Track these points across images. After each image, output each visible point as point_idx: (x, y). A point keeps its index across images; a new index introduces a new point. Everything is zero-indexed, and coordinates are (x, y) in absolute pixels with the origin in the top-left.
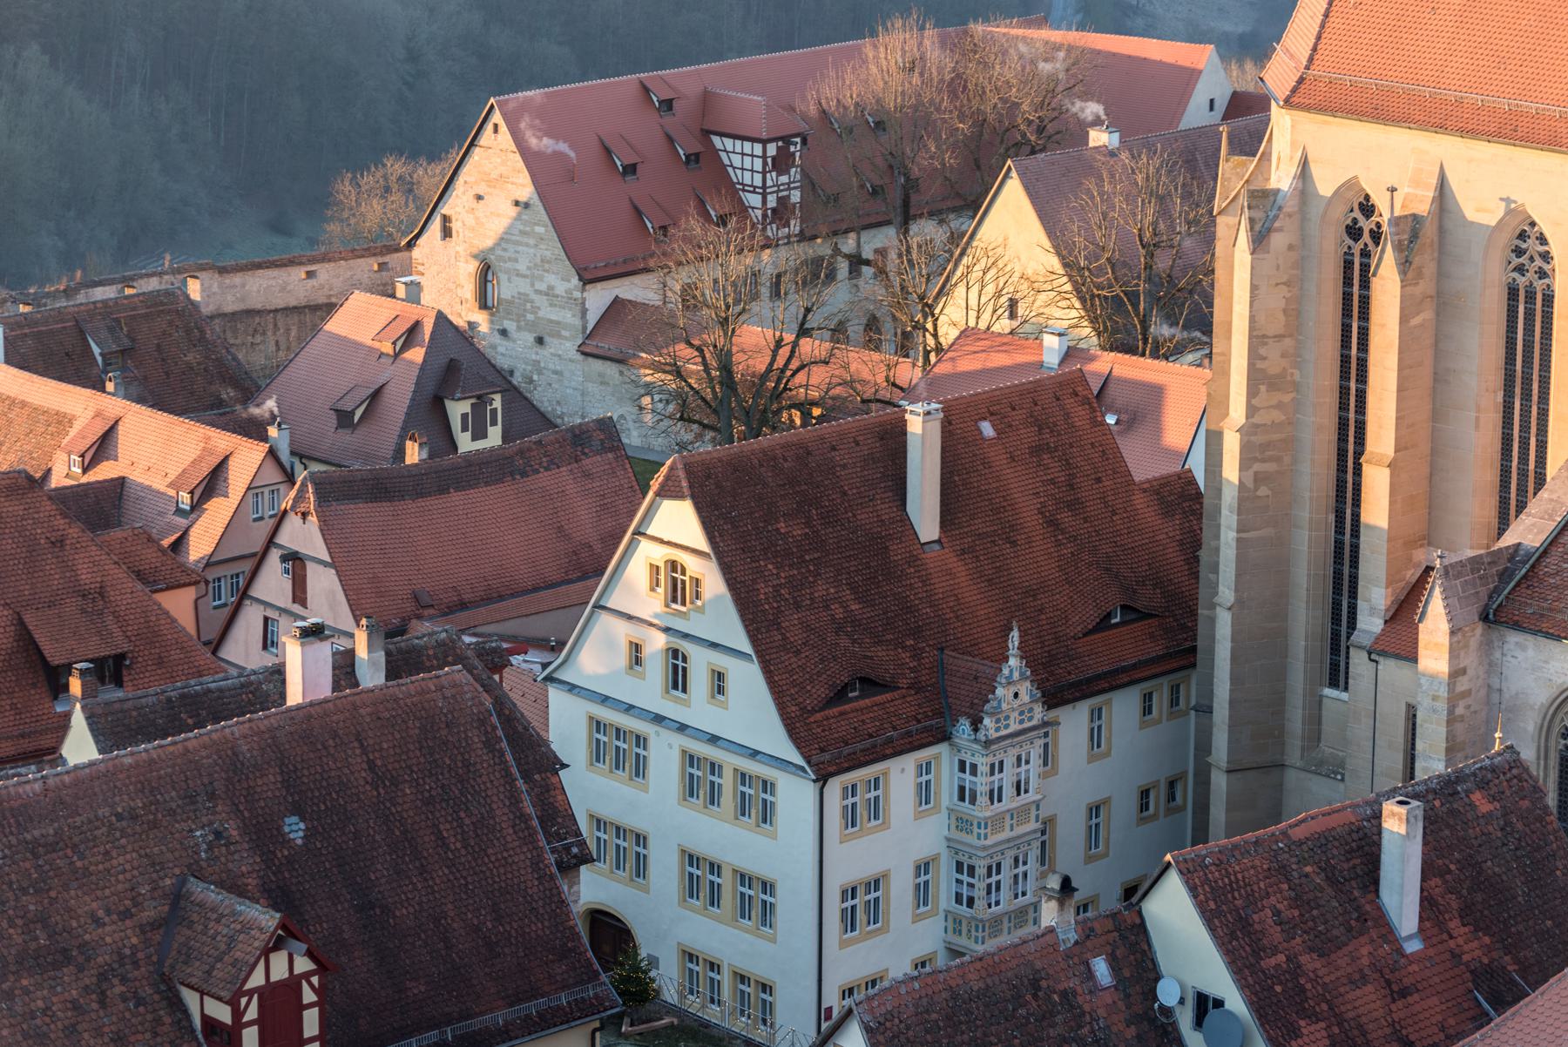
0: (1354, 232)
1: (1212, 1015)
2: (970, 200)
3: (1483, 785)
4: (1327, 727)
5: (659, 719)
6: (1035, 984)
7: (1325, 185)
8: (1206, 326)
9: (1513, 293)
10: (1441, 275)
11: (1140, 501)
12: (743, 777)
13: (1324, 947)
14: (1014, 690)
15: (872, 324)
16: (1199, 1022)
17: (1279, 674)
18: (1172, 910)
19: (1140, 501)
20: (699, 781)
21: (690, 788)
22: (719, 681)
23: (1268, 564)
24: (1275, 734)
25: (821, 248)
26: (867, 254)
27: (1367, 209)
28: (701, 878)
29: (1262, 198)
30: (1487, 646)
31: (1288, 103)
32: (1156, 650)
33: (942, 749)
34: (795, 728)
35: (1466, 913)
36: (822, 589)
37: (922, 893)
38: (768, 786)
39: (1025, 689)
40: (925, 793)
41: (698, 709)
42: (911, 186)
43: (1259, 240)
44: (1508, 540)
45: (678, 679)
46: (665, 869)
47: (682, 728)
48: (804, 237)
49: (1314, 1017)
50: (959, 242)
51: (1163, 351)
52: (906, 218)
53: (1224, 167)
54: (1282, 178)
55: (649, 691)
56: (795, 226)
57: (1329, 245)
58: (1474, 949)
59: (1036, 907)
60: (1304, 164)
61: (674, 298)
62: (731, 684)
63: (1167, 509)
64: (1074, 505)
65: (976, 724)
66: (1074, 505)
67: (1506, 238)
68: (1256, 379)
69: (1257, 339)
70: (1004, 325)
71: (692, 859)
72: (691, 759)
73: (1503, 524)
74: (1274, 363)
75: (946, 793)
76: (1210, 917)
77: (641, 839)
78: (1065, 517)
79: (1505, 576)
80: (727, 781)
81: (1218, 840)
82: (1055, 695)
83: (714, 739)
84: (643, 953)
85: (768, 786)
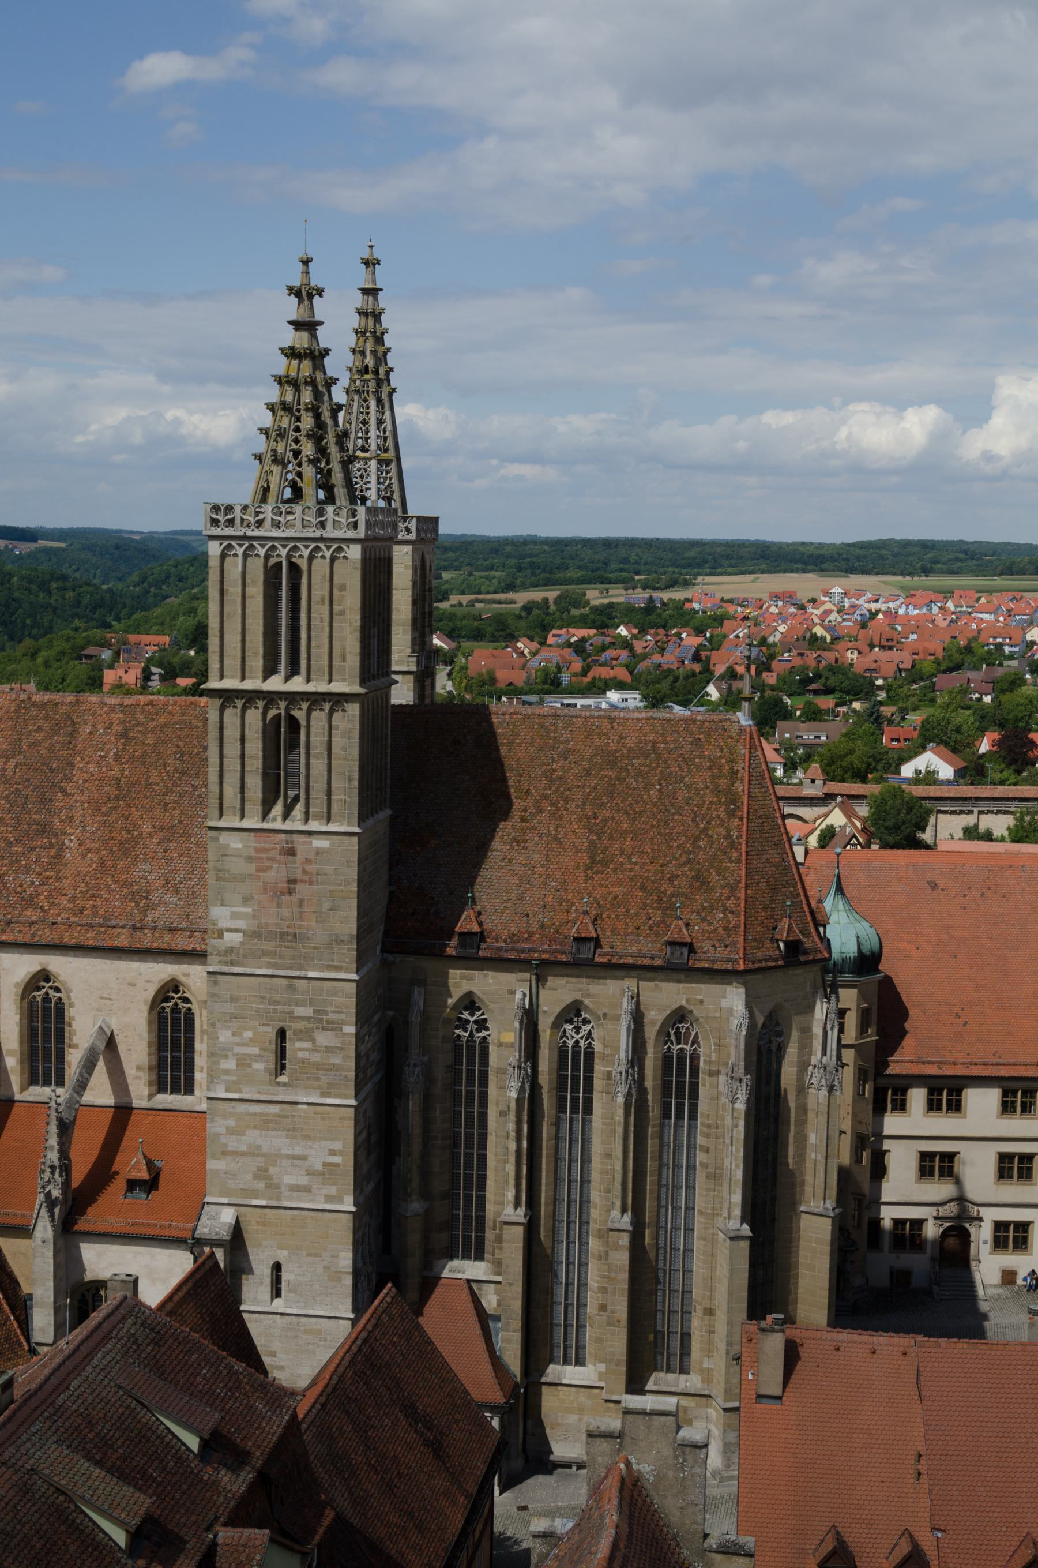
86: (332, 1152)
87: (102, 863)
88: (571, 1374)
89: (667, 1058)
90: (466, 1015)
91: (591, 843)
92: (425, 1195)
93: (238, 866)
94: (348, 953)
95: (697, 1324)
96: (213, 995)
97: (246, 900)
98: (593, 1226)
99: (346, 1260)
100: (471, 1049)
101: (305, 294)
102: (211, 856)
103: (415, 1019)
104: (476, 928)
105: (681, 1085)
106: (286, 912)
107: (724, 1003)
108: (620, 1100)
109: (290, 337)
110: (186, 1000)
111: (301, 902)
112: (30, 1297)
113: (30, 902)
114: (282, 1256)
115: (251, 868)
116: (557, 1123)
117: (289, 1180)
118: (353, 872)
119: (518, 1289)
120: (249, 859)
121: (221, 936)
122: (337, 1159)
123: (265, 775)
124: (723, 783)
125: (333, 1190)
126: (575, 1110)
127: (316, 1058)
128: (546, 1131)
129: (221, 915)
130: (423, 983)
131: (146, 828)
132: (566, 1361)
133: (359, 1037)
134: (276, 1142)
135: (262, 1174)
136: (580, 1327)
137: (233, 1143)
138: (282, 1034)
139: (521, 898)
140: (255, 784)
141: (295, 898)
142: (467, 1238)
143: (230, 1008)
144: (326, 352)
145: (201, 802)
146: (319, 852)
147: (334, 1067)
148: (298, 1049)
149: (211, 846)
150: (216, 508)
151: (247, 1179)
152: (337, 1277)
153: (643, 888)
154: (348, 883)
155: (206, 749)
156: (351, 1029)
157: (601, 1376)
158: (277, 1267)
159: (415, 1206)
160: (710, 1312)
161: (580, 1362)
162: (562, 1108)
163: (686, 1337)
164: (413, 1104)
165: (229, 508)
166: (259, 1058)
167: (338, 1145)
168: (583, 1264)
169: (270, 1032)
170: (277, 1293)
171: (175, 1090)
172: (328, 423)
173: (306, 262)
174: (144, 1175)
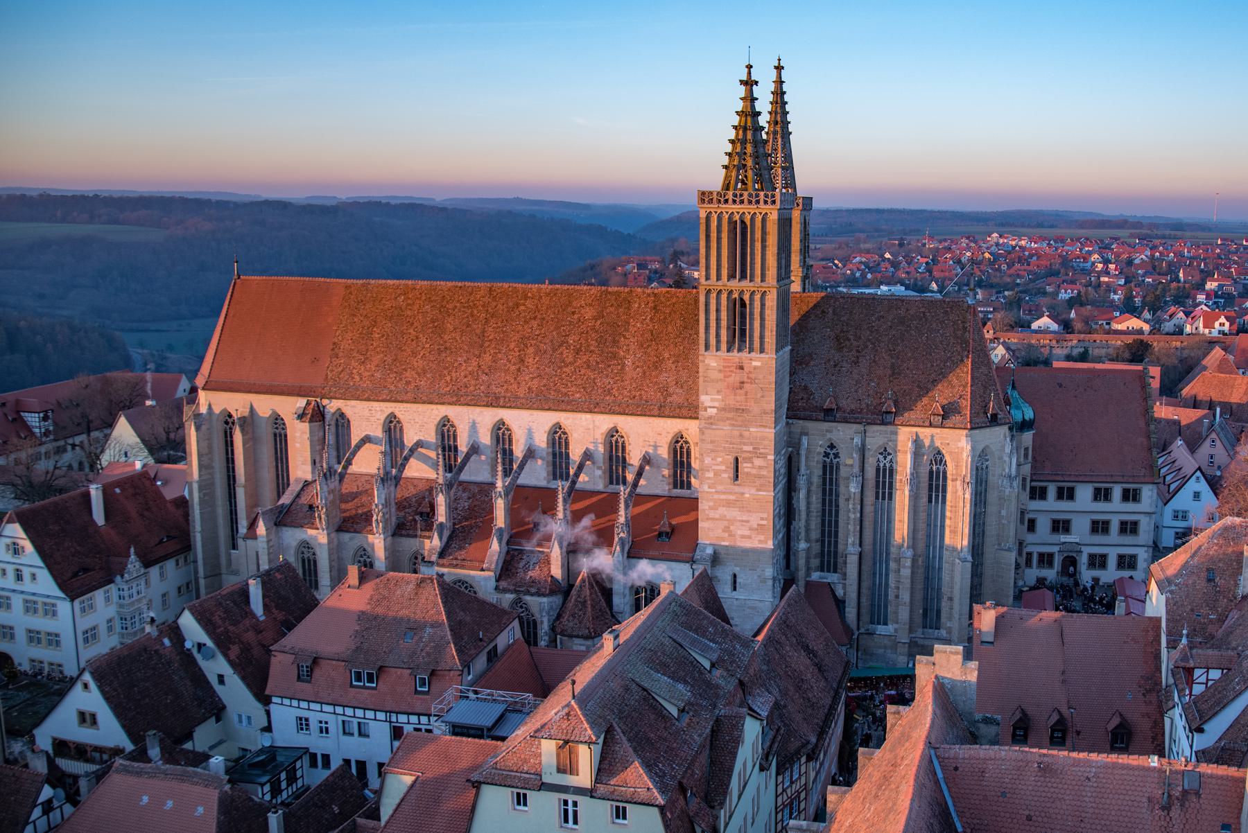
0: (227, 423)
1: (203, 648)
2: (111, 425)
3: (278, 571)
4: (233, 561)
5: (14, 591)
6: (145, 650)
7: (217, 410)
8: (185, 452)
9: (275, 435)
10: (253, 432)
11: (169, 505)
12: (45, 604)
13: (236, 623)
14: (133, 564)
15: (81, 463)
16: (199, 651)
17: (217, 549)
18: (188, 622)
19: (169, 505)
20: (30, 607)
21: (27, 610)
22: (34, 576)
23: (209, 518)
24: (218, 566)
25: (61, 443)
26: (77, 442)
27: (230, 416)
28: (34, 636)
29: (197, 416)
30: (277, 532)
31: (203, 389)
32: (178, 547)
33: (112, 585)
34: (61, 586)
35: (277, 607)
36: (66, 544)
37: (110, 629)
38: (54, 605)
39: (138, 564)
40: (108, 599)
41: (27, 585)
42: (89, 422)
43: (198, 429)
44: (281, 502)
45: (19, 577)
46: (21, 635)
47: (22, 592)
48: (55, 440)
49: (234, 643)
50: (107, 437)
51: (175, 461)
52: (89, 432)
53: (186, 409)
54: (203, 410)
55: (10, 582)
56: (52, 437)
57: (219, 428)
58: (280, 616)
59: (143, 629)
60: (210, 406)
61: (12, 464)
62: (38, 576)
63: (178, 507)
64: (148, 509)
65: (122, 576)
66: (148, 509)
67: (272, 420)
68: (201, 467)
69: (200, 455)
70: (123, 459)
71: (30, 631)
72: (26, 601)
73: (279, 497)
74: (206, 461)
75: (115, 598)
76: (199, 621)
77: (11, 628)
78: (146, 513)
79: (280, 512)
80: (40, 606)
81: (203, 596)
82: (147, 564)
83: (34, 594)
84: (16, 663)
85: (54, 605)
86: (762, 519)
87: (644, 373)
88: (881, 629)
89: (931, 472)
90: (829, 450)
91: (893, 364)
92: (808, 540)
93: (715, 375)
94: (770, 419)
95: (945, 605)
96: (702, 440)
97: (719, 392)
98: (892, 556)
99: (769, 572)
100: (831, 467)
101: (749, 83)
102: (700, 370)
103: (803, 452)
104: (834, 406)
105: (937, 486)
106: (738, 398)
107: (960, 445)
108: (907, 493)
109: (740, 106)
110: (687, 442)
111: (746, 394)
112: (611, 590)
113: (609, 393)
114: (737, 570)
115: (721, 376)
116: (875, 505)
117: (740, 532)
118: (773, 378)
119: (855, 587)
120: (720, 371)
121: (706, 410)
122: (764, 522)
123: (728, 328)
124: (959, 333)
125: (762, 538)
126: (884, 498)
127: (754, 471)
128: (869, 509)
129: (705, 399)
130: (807, 434)
131: (666, 355)
132: (879, 623)
133: (776, 462)
134: (733, 513)
135: (726, 529)
136: (886, 607)
137: (712, 514)
138: (737, 459)
139: (856, 391)
140: (724, 332)
141: (742, 392)
142: (829, 562)
143: (710, 446)
144: (759, 114)
145: (695, 342)
146: (755, 368)
147: (760, 477)
148: (745, 467)
149: (701, 365)
150: (703, 193)
151: (719, 532)
152: (764, 581)
153: (918, 386)
154: (770, 383)
155: (697, 315)
156: (772, 457)
157: (896, 630)
158: (735, 576)
159: (803, 545)
160: (951, 599)
161: (886, 624)
162: (877, 498)
163: (939, 612)
164: (802, 494)
165: (711, 193)
166: (725, 471)
167: (765, 515)
168: (887, 575)
169: (731, 459)
170: (735, 589)
171: (682, 487)
172: (761, 147)
173: (749, 67)
174: (668, 530)
